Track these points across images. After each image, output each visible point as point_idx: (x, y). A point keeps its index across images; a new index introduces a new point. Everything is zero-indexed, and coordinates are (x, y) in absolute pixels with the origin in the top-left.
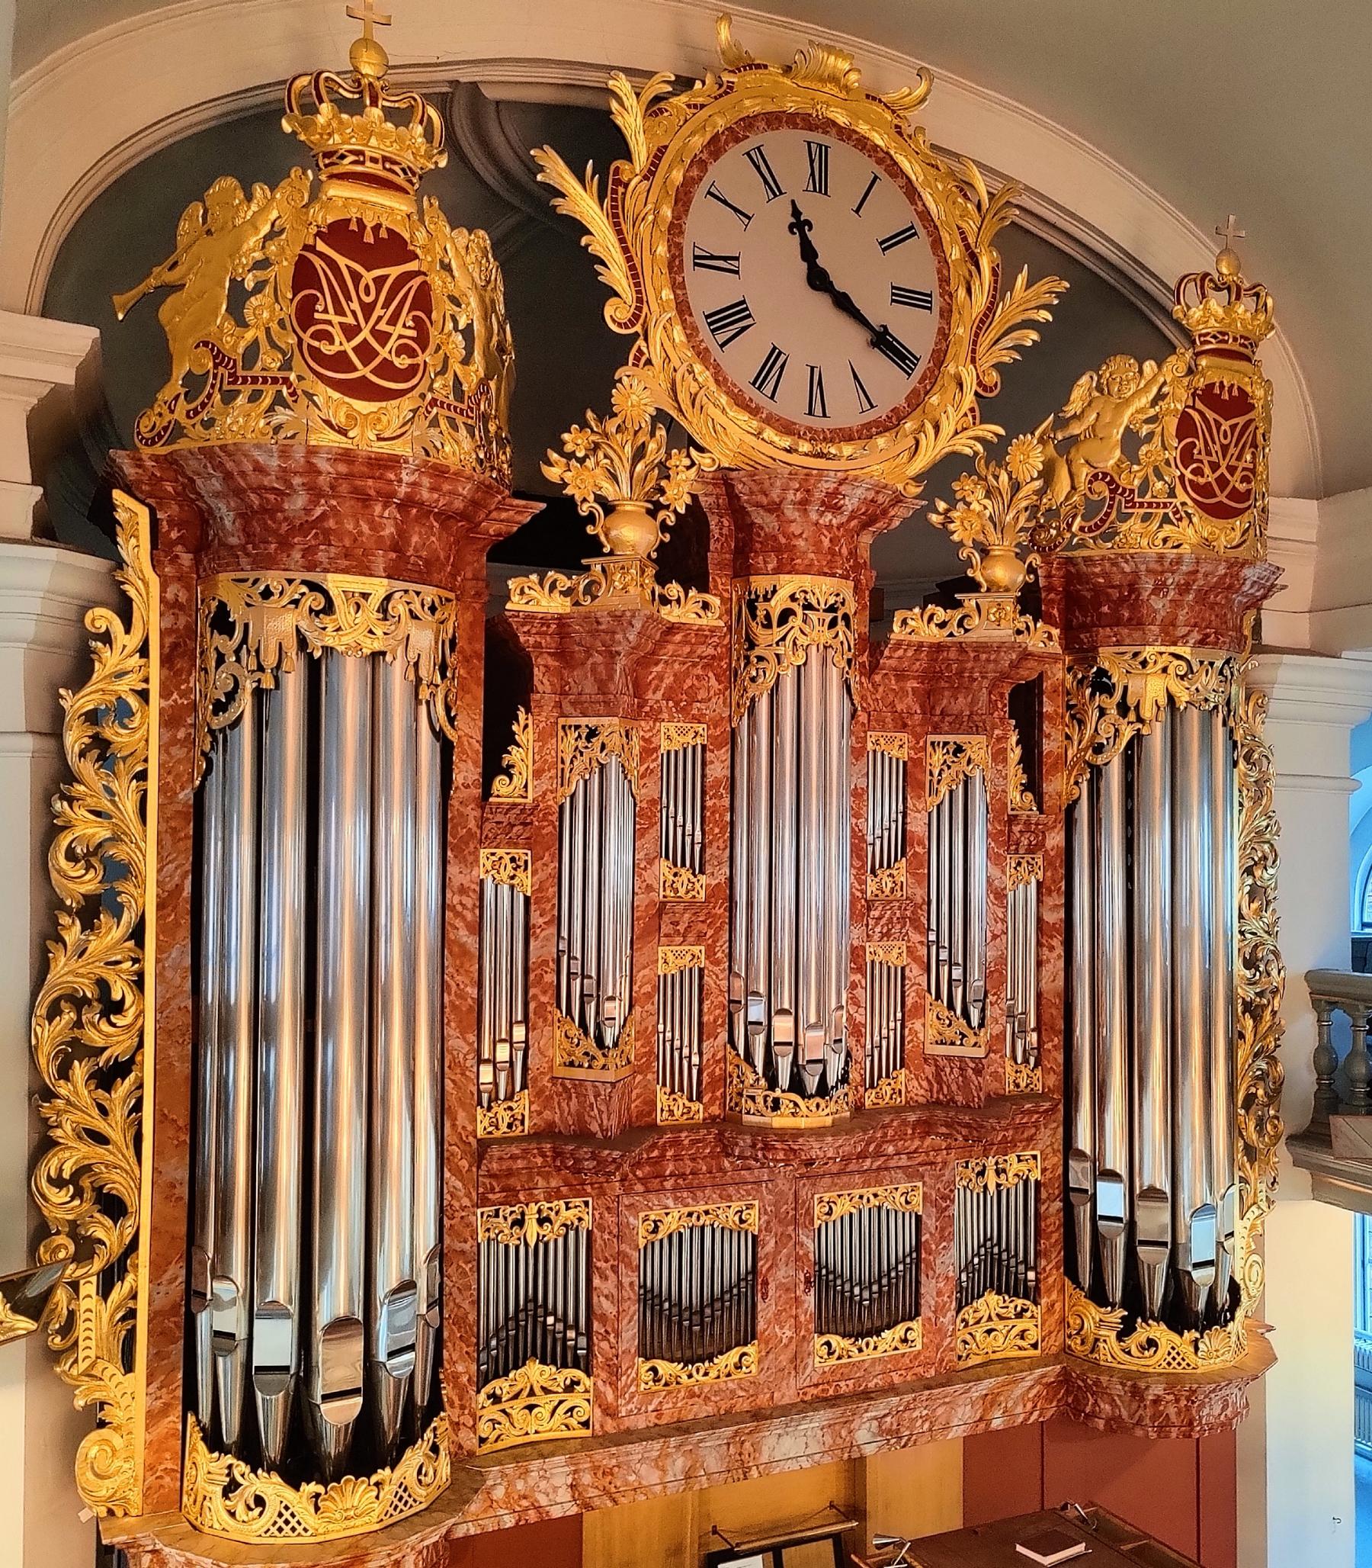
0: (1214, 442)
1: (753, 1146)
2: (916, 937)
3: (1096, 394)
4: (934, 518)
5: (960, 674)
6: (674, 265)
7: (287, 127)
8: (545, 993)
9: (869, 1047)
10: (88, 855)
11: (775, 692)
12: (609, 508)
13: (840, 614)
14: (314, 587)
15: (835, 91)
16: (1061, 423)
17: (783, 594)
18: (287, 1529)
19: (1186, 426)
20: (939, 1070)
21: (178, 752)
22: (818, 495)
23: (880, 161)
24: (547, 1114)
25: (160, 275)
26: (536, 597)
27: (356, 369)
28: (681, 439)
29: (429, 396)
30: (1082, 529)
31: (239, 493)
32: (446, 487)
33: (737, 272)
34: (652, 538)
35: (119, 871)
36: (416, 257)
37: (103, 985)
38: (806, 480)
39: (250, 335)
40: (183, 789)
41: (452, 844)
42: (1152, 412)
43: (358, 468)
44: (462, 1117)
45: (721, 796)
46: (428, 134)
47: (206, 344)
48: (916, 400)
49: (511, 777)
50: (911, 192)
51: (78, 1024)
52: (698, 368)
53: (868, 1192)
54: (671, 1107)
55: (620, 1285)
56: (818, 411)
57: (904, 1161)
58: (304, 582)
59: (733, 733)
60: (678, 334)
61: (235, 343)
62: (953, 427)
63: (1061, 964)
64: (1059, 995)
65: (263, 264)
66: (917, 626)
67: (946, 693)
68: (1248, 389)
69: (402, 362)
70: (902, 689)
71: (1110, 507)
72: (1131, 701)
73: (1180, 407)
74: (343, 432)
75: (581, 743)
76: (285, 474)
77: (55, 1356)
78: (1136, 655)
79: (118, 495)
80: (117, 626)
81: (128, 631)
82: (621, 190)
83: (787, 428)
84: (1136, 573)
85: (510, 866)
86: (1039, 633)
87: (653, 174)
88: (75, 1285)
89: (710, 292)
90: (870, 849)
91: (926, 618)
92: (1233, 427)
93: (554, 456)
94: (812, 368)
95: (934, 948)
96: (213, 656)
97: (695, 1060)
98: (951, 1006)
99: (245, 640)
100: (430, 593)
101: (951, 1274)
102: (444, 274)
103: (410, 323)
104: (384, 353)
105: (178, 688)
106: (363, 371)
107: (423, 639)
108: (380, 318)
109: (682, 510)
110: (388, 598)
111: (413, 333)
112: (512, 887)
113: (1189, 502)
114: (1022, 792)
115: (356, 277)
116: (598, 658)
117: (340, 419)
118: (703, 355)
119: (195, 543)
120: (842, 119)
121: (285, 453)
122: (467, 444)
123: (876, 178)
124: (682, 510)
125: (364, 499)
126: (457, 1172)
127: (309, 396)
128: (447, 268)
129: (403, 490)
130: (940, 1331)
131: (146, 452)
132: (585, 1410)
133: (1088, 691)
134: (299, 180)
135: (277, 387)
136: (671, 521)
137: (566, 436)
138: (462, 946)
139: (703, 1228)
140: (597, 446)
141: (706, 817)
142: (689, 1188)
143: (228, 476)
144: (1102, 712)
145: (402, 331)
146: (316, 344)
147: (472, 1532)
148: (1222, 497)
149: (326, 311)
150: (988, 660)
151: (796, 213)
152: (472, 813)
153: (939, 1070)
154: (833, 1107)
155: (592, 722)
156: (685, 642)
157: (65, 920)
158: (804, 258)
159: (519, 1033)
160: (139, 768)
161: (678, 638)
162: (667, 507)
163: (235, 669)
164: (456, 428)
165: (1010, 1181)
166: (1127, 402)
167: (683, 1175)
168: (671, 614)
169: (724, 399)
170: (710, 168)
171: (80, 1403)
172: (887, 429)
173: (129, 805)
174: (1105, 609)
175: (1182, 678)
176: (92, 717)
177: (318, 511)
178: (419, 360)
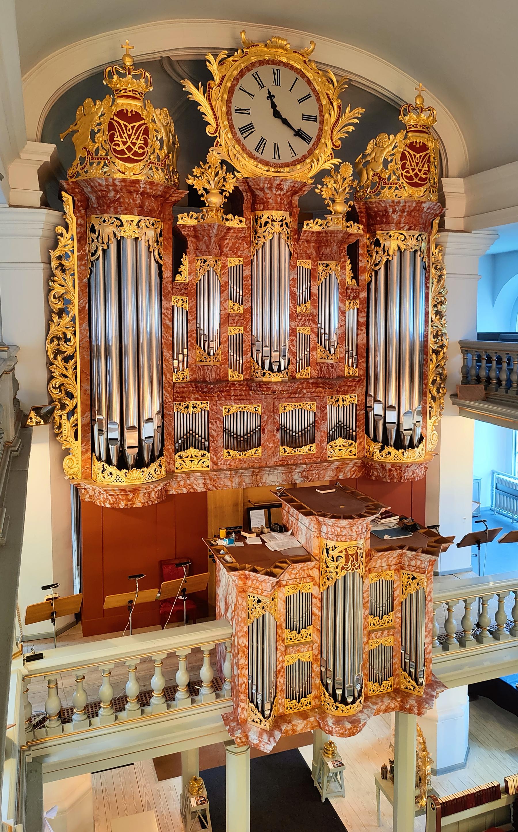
0: (413, 162)
1: (257, 386)
2: (314, 326)
3: (375, 146)
4: (317, 191)
5: (327, 241)
6: (228, 113)
7: (105, 83)
8: (193, 340)
9: (298, 359)
10: (59, 297)
11: (263, 247)
12: (207, 191)
13: (284, 223)
14: (118, 219)
15: (282, 51)
16: (365, 156)
17: (265, 216)
18: (118, 481)
19: (403, 157)
20: (321, 367)
21: (83, 268)
22: (275, 185)
23: (298, 73)
24: (194, 376)
25: (73, 128)
26: (187, 220)
27: (127, 154)
28: (231, 169)
29: (149, 161)
30: (370, 192)
31: (95, 192)
32: (155, 188)
33: (249, 114)
34: (221, 201)
35: (68, 302)
36: (143, 119)
37: (64, 334)
38: (270, 181)
39: (97, 145)
40: (85, 278)
42: (392, 152)
43: (128, 184)
44: (168, 376)
45: (248, 281)
46: (146, 82)
47: (85, 148)
48: (311, 152)
49: (181, 275)
50: (309, 82)
51: (58, 345)
52: (236, 146)
53: (297, 404)
54: (233, 376)
55: (217, 427)
56: (277, 157)
57: (309, 395)
58: (114, 218)
59: (252, 261)
60: (230, 135)
61: (93, 148)
62: (325, 160)
63: (365, 335)
64: (364, 345)
65: (99, 124)
66: (312, 226)
67: (324, 247)
68: (426, 143)
69: (140, 151)
70: (309, 246)
71: (379, 184)
72: (386, 249)
73: (402, 150)
74: (124, 173)
75: (202, 264)
76: (107, 186)
77: (57, 435)
78: (388, 234)
79: (63, 193)
80: (64, 232)
81: (67, 233)
82: (211, 90)
83: (267, 164)
84: (386, 206)
85: (181, 302)
86: (355, 227)
87: (221, 84)
88: (61, 416)
89: (240, 121)
90: (298, 298)
91: (315, 223)
92: (420, 156)
93: (190, 177)
94: (275, 144)
95: (320, 329)
96: (91, 239)
97: (241, 361)
98: (325, 347)
99: (99, 235)
100: (152, 220)
101: (326, 431)
102: (153, 123)
103: (142, 139)
104: (135, 149)
105: (82, 249)
106: (129, 155)
107: (151, 234)
108: (133, 138)
109: (231, 192)
110: (139, 221)
111: (143, 142)
112: (182, 308)
113: (405, 183)
114: (351, 279)
115: (126, 127)
116: (206, 238)
117: (122, 169)
118: (238, 142)
119: (85, 207)
120: (284, 60)
121: (107, 180)
122: (162, 174)
123: (297, 79)
124: (231, 192)
125: (131, 193)
126: (167, 391)
127: (113, 163)
128: (154, 121)
129: (141, 190)
130: (322, 448)
131: (70, 180)
132: (208, 463)
133: (373, 246)
134: (109, 98)
135: (104, 161)
136: (228, 195)
137: (194, 170)
138: (168, 325)
139: (244, 412)
140: (203, 173)
141: (244, 288)
142: (239, 399)
143: (92, 187)
144: (377, 253)
145: (140, 142)
146: (115, 147)
147: (174, 493)
148: (416, 180)
149: (117, 137)
150: (334, 236)
151: (269, 93)
152: (170, 286)
153: (321, 367)
154: (282, 376)
155: (205, 258)
156: (234, 232)
157: (54, 315)
158: (272, 108)
159: (185, 351)
160: (72, 272)
161: (232, 231)
162: (226, 191)
163: (97, 243)
164: (158, 170)
165: (347, 404)
166: (385, 149)
167: (237, 396)
168: (229, 224)
169: (245, 156)
170: (240, 81)
171: (63, 448)
172: (301, 162)
173: (70, 283)
174: (378, 219)
175: (403, 241)
176: (59, 258)
177: (118, 197)
178: (145, 150)
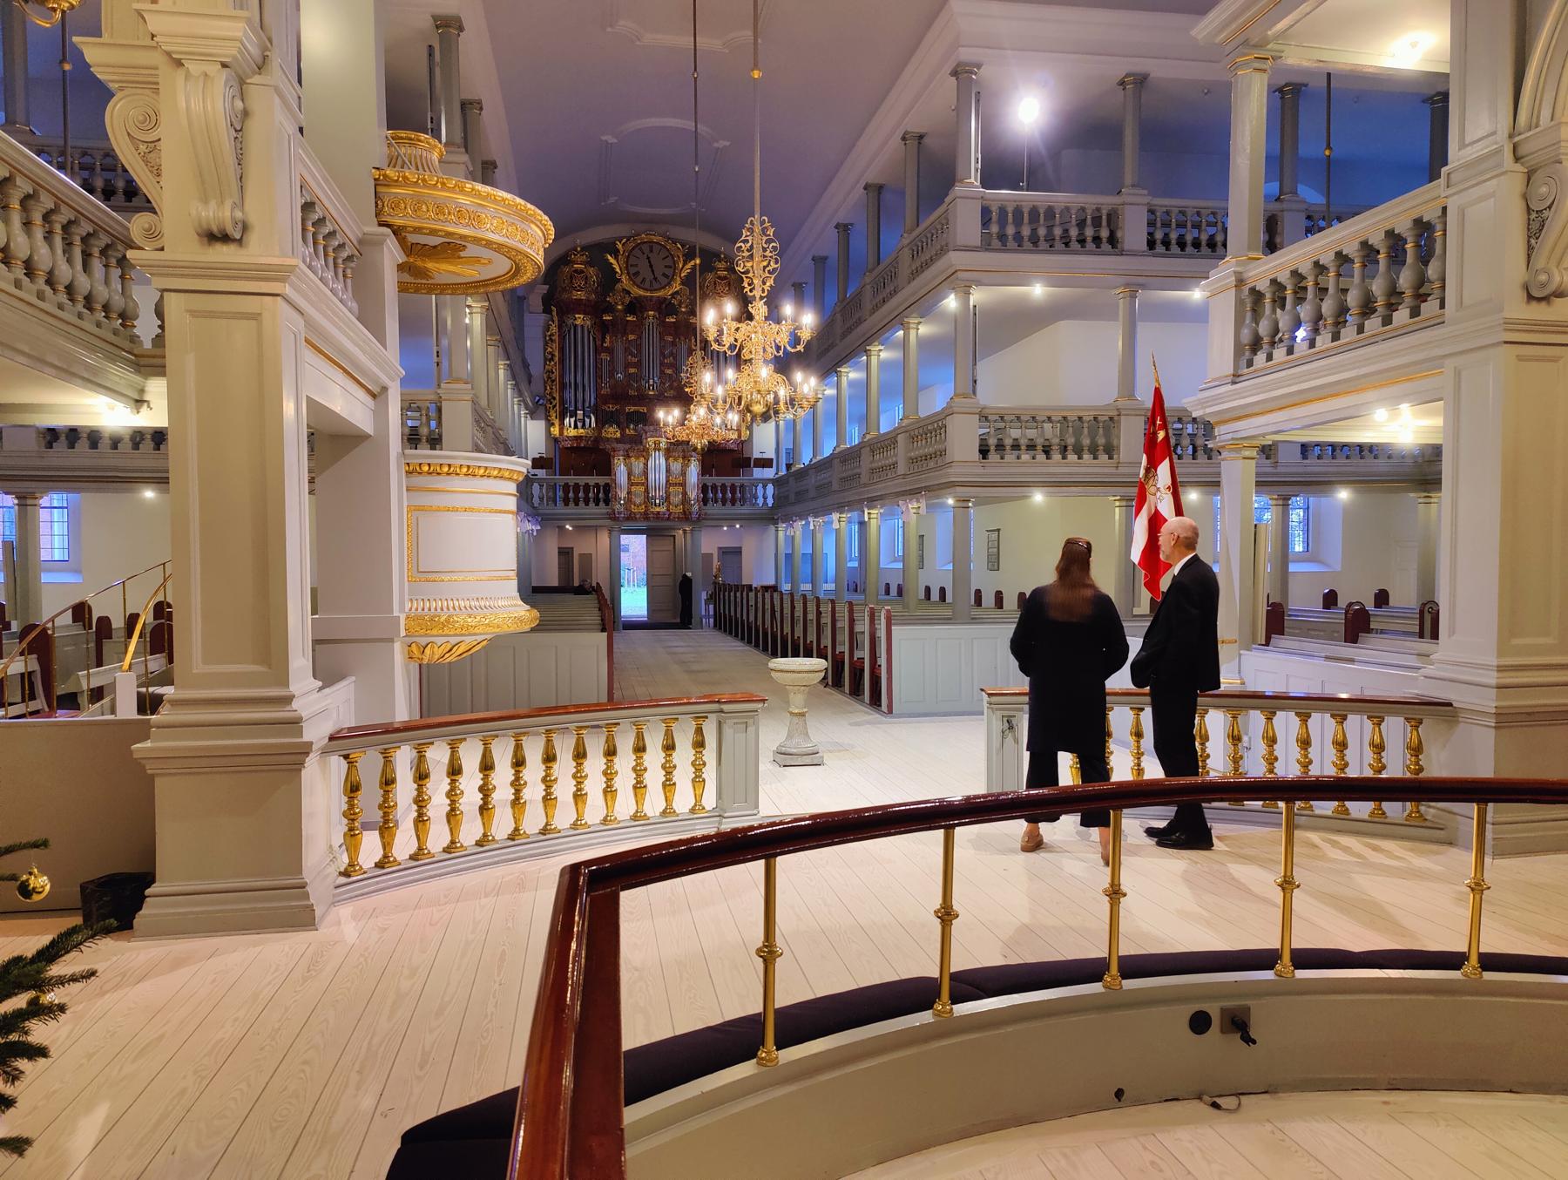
26: (607, 318)
28: (628, 293)
41: (596, 352)
54: (632, 393)
89: (633, 270)
